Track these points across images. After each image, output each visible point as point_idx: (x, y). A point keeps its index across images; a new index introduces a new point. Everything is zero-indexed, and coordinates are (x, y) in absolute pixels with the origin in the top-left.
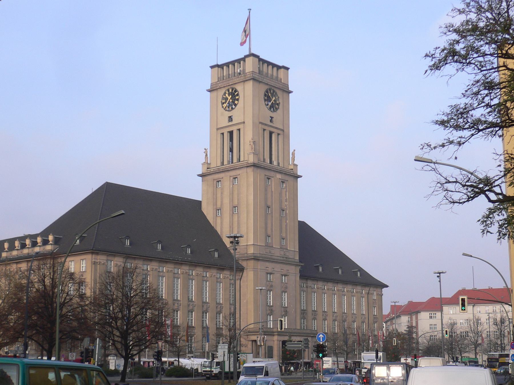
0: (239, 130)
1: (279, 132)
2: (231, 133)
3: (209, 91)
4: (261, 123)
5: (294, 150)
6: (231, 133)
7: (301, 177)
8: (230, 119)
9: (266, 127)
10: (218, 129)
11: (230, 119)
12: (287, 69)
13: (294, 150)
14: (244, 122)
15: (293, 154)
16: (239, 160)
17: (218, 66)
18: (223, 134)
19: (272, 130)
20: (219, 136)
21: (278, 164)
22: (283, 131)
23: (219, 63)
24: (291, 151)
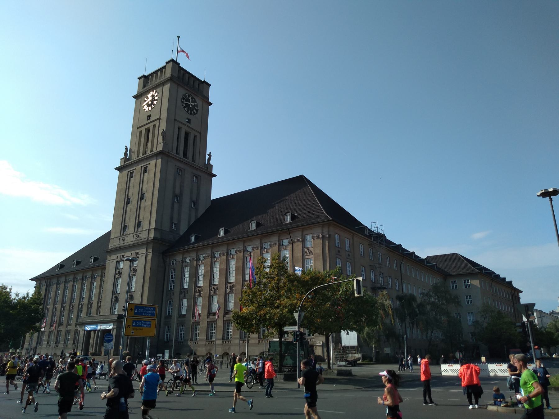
0: (154, 126)
2: (148, 130)
3: (135, 97)
4: (175, 120)
7: (215, 176)
9: (181, 125)
12: (209, 85)
14: (159, 119)
16: (152, 151)
17: (144, 76)
18: (141, 132)
19: (189, 130)
21: (193, 161)
22: (200, 133)
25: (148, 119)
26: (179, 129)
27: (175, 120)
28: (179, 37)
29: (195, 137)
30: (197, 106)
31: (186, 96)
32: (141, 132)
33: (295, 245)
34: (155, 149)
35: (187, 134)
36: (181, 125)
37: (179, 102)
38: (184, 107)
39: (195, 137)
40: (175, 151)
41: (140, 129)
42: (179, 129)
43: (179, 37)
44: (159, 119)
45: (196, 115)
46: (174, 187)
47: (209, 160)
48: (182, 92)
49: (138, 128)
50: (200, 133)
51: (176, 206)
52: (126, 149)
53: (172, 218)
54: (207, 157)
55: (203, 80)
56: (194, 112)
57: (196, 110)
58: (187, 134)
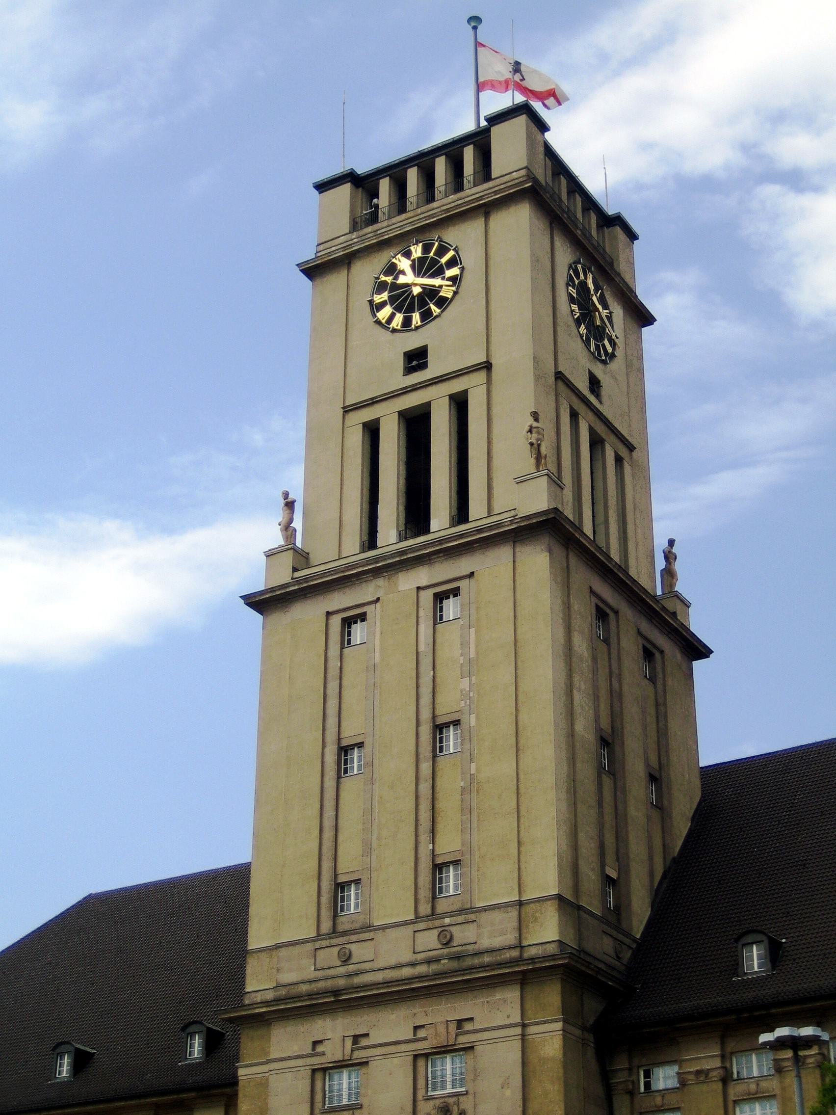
1: (623, 452)
2: (416, 425)
4: (559, 376)
5: (671, 543)
6: (416, 425)
8: (416, 359)
10: (347, 410)
11: (416, 359)
13: (671, 543)
14: (487, 366)
15: (669, 557)
17: (351, 177)
18: (372, 431)
20: (356, 439)
23: (362, 169)
24: (660, 544)
25: (409, 370)
28: (475, 21)
32: (372, 431)
34: (477, 508)
41: (367, 415)
43: (475, 21)
44: (487, 366)
47: (669, 574)
49: (347, 410)
52: (290, 505)
54: (660, 563)
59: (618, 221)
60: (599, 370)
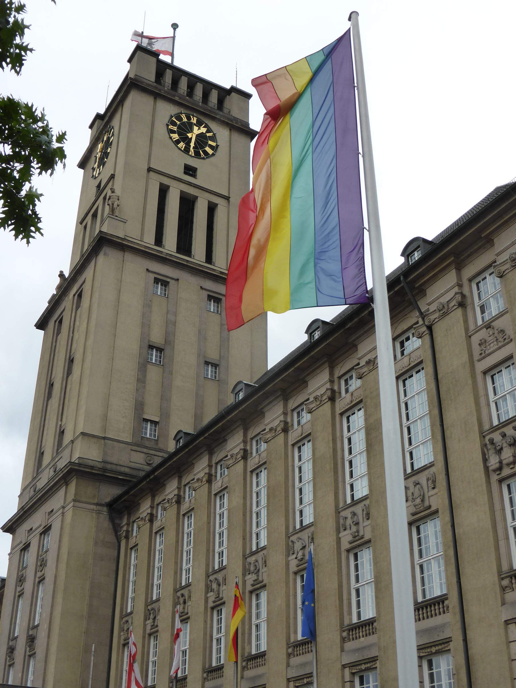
4: (150, 170)
17: (98, 117)
18: (85, 227)
22: (227, 198)
26: (163, 191)
27: (150, 170)
29: (212, 209)
30: (213, 138)
31: (179, 118)
33: (439, 330)
35: (187, 204)
36: (166, 181)
37: (161, 129)
38: (177, 142)
39: (212, 209)
40: (150, 239)
42: (163, 191)
44: (112, 177)
45: (212, 159)
46: (146, 325)
48: (166, 110)
50: (227, 198)
51: (153, 374)
53: (139, 406)
55: (228, 87)
56: (206, 153)
57: (211, 147)
58: (187, 204)
59: (234, 90)
60: (193, 162)
